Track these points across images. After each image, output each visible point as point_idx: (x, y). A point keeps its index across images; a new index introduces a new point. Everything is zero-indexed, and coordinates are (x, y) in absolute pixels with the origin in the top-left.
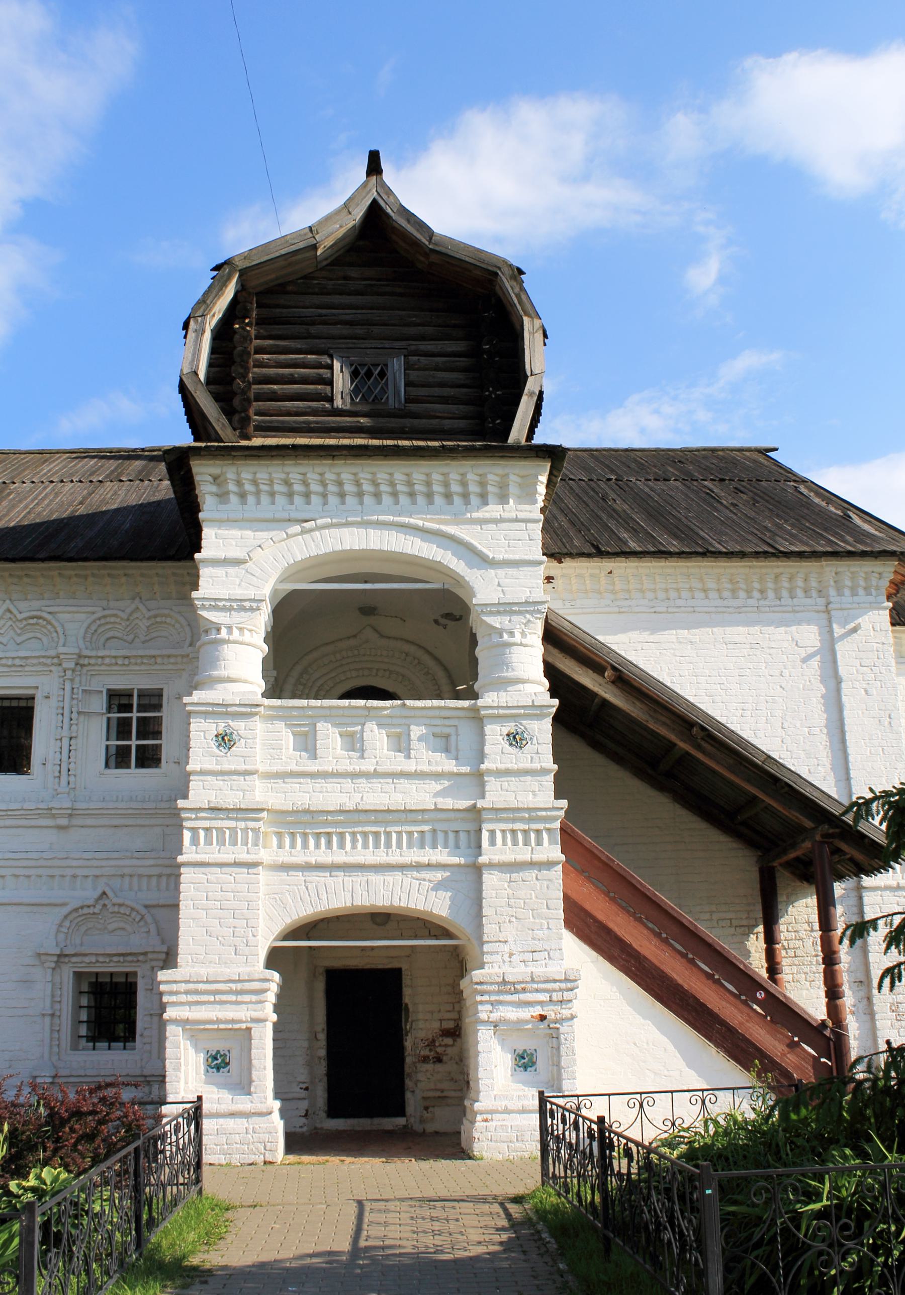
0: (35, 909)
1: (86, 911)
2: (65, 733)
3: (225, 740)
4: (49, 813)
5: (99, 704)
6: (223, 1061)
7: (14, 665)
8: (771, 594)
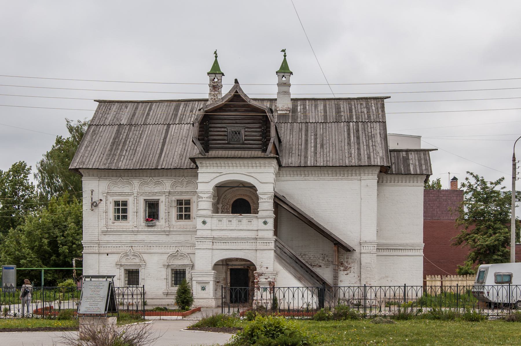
3: (204, 223)
4: (164, 231)
8: (346, 175)
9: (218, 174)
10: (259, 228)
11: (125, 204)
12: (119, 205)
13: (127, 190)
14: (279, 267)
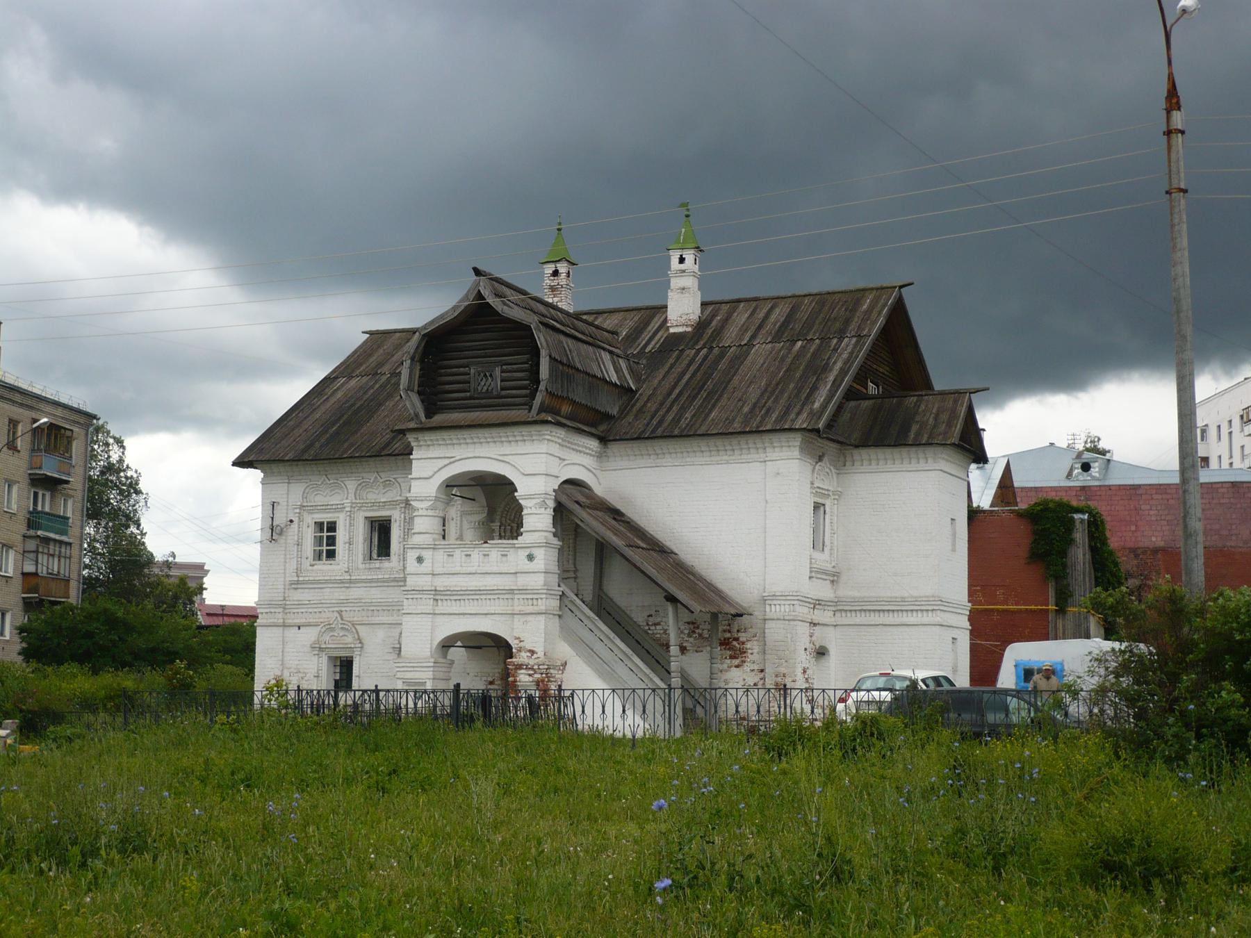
3: (420, 560)
9: (447, 461)
10: (519, 569)
11: (332, 527)
12: (322, 530)
13: (335, 500)
14: (564, 650)
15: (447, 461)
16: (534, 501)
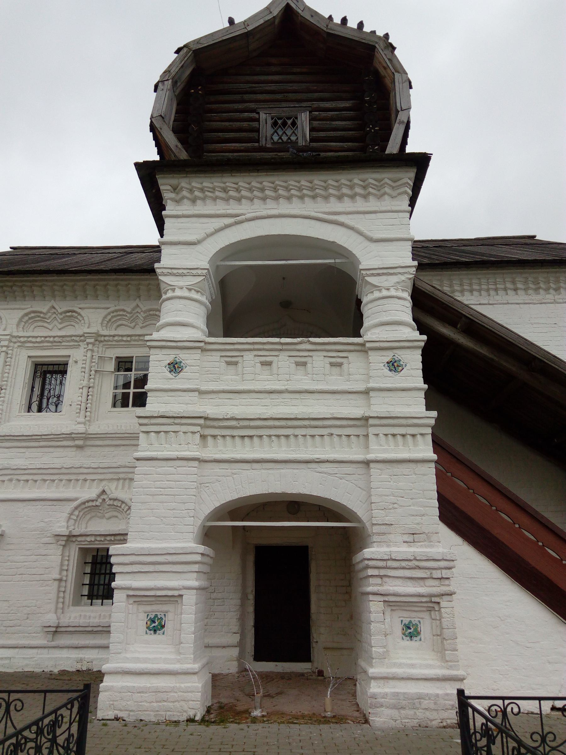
0: (55, 503)
1: (90, 504)
2: (85, 383)
4: (70, 436)
5: (111, 366)
6: (160, 623)
7: (55, 342)
9: (231, 220)
15: (231, 220)
16: (393, 279)
